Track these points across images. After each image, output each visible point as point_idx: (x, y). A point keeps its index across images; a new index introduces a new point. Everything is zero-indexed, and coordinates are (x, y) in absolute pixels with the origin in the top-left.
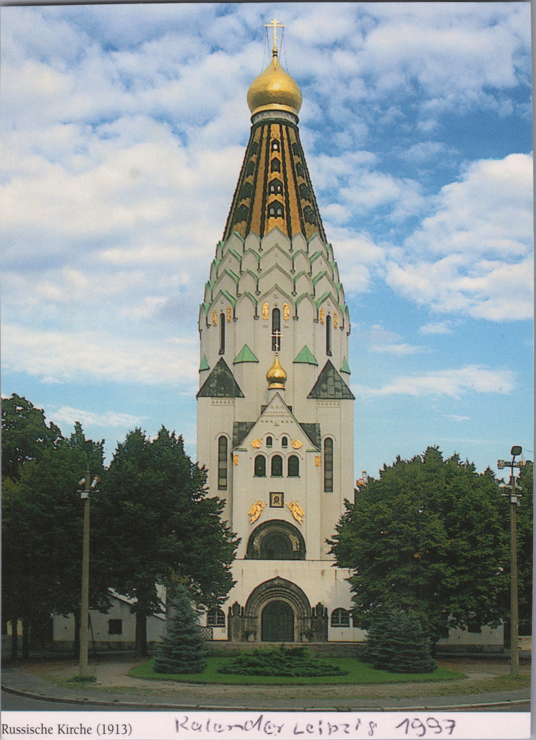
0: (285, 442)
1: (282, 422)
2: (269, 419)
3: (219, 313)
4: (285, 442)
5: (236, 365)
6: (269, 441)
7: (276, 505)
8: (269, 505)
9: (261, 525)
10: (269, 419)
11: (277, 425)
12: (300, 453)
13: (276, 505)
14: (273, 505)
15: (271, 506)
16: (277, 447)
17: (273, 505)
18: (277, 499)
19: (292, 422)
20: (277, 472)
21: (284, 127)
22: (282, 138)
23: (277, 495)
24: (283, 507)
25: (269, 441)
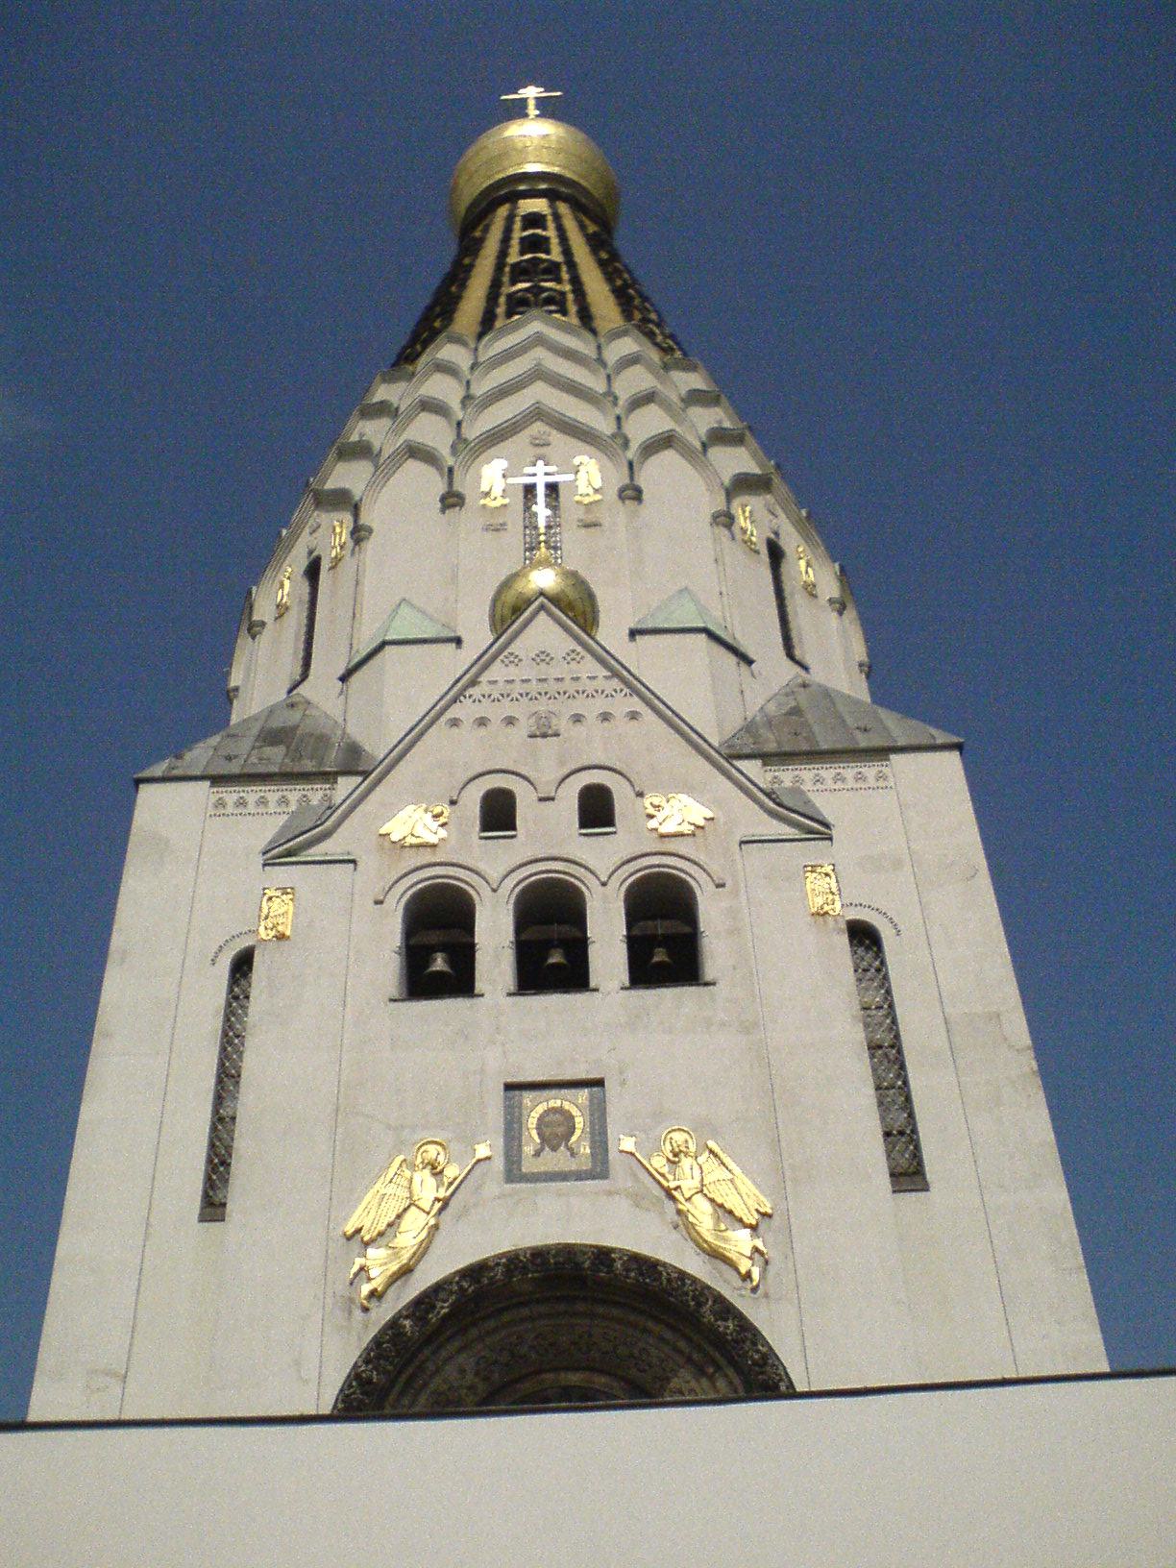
0: (596, 809)
1: (577, 719)
2: (495, 712)
3: (304, 563)
4: (596, 809)
5: (356, 679)
6: (498, 813)
7: (556, 1160)
8: (499, 1164)
9: (438, 1288)
10: (495, 712)
11: (544, 732)
12: (702, 858)
13: (556, 1160)
14: (529, 1166)
15: (513, 1172)
16: (548, 832)
17: (529, 1166)
18: (554, 1120)
19: (634, 716)
20: (551, 956)
21: (563, 208)
22: (557, 217)
23: (555, 1100)
24: (603, 1174)
25: (498, 813)
